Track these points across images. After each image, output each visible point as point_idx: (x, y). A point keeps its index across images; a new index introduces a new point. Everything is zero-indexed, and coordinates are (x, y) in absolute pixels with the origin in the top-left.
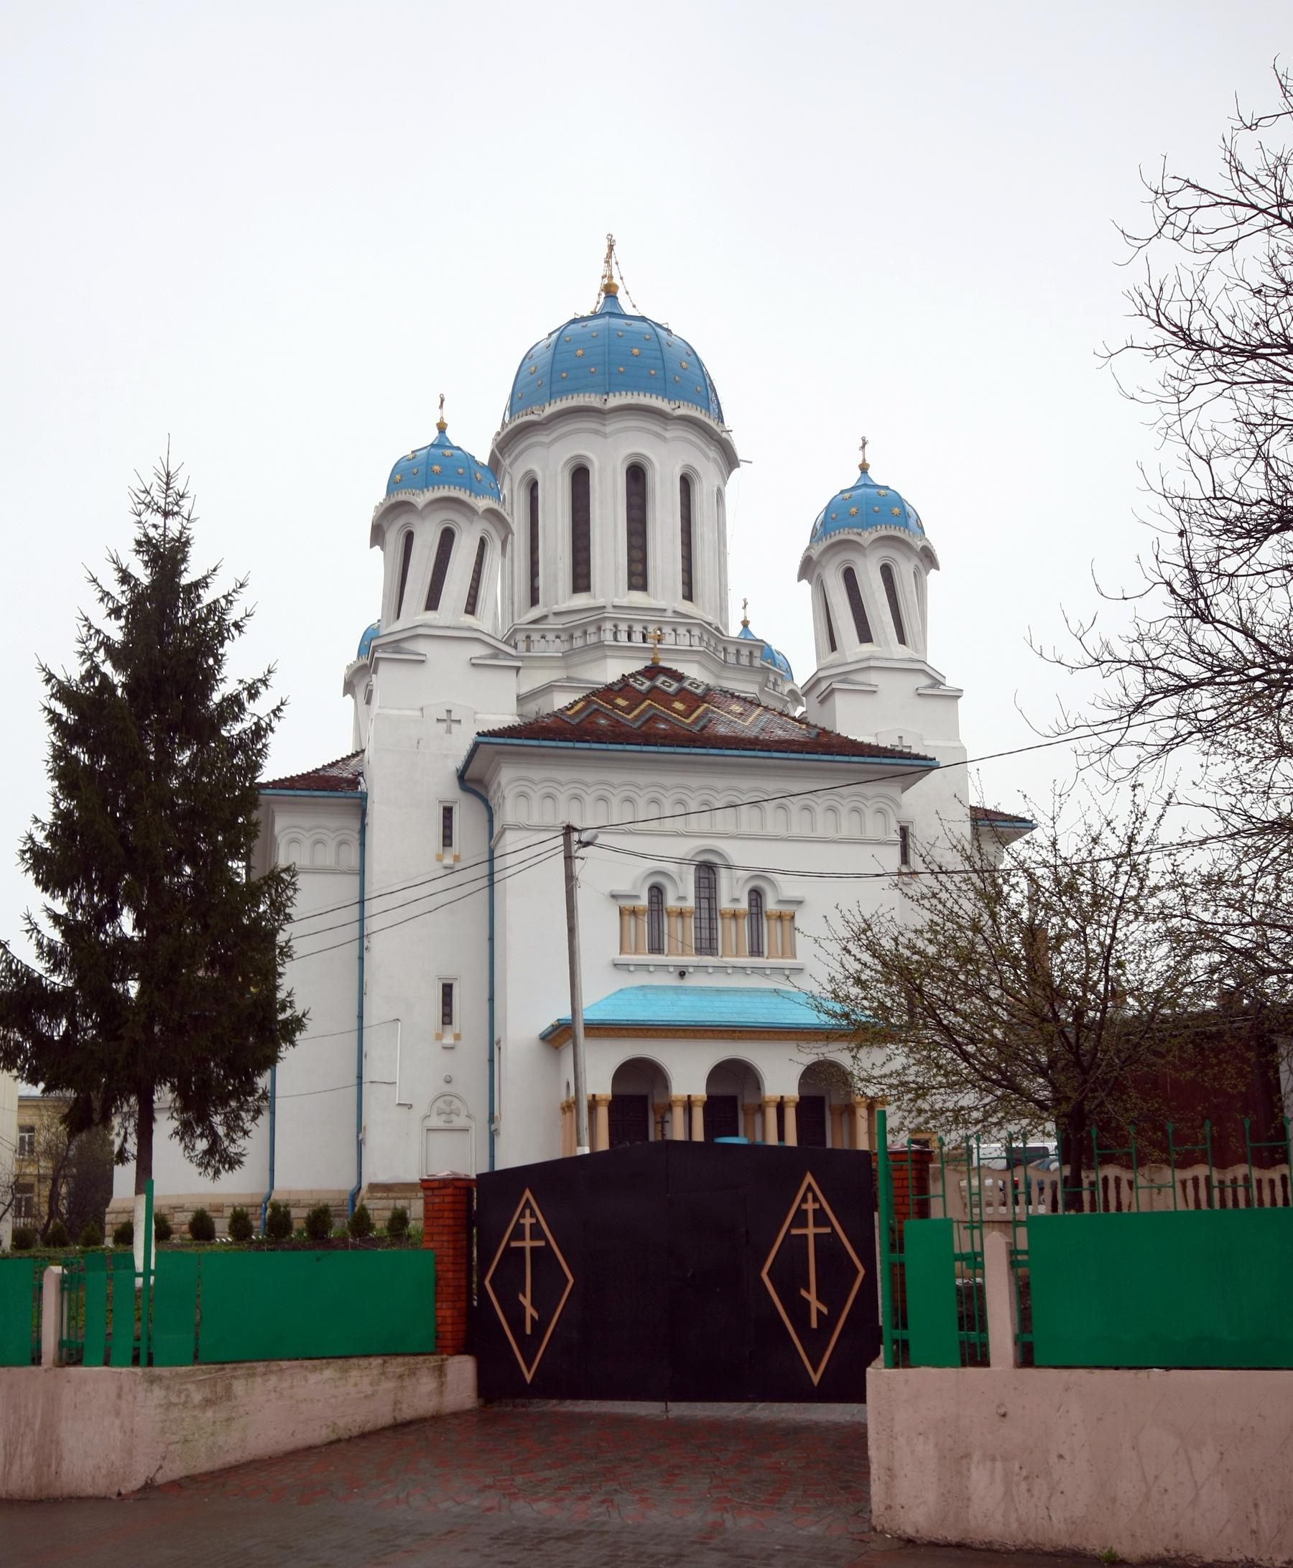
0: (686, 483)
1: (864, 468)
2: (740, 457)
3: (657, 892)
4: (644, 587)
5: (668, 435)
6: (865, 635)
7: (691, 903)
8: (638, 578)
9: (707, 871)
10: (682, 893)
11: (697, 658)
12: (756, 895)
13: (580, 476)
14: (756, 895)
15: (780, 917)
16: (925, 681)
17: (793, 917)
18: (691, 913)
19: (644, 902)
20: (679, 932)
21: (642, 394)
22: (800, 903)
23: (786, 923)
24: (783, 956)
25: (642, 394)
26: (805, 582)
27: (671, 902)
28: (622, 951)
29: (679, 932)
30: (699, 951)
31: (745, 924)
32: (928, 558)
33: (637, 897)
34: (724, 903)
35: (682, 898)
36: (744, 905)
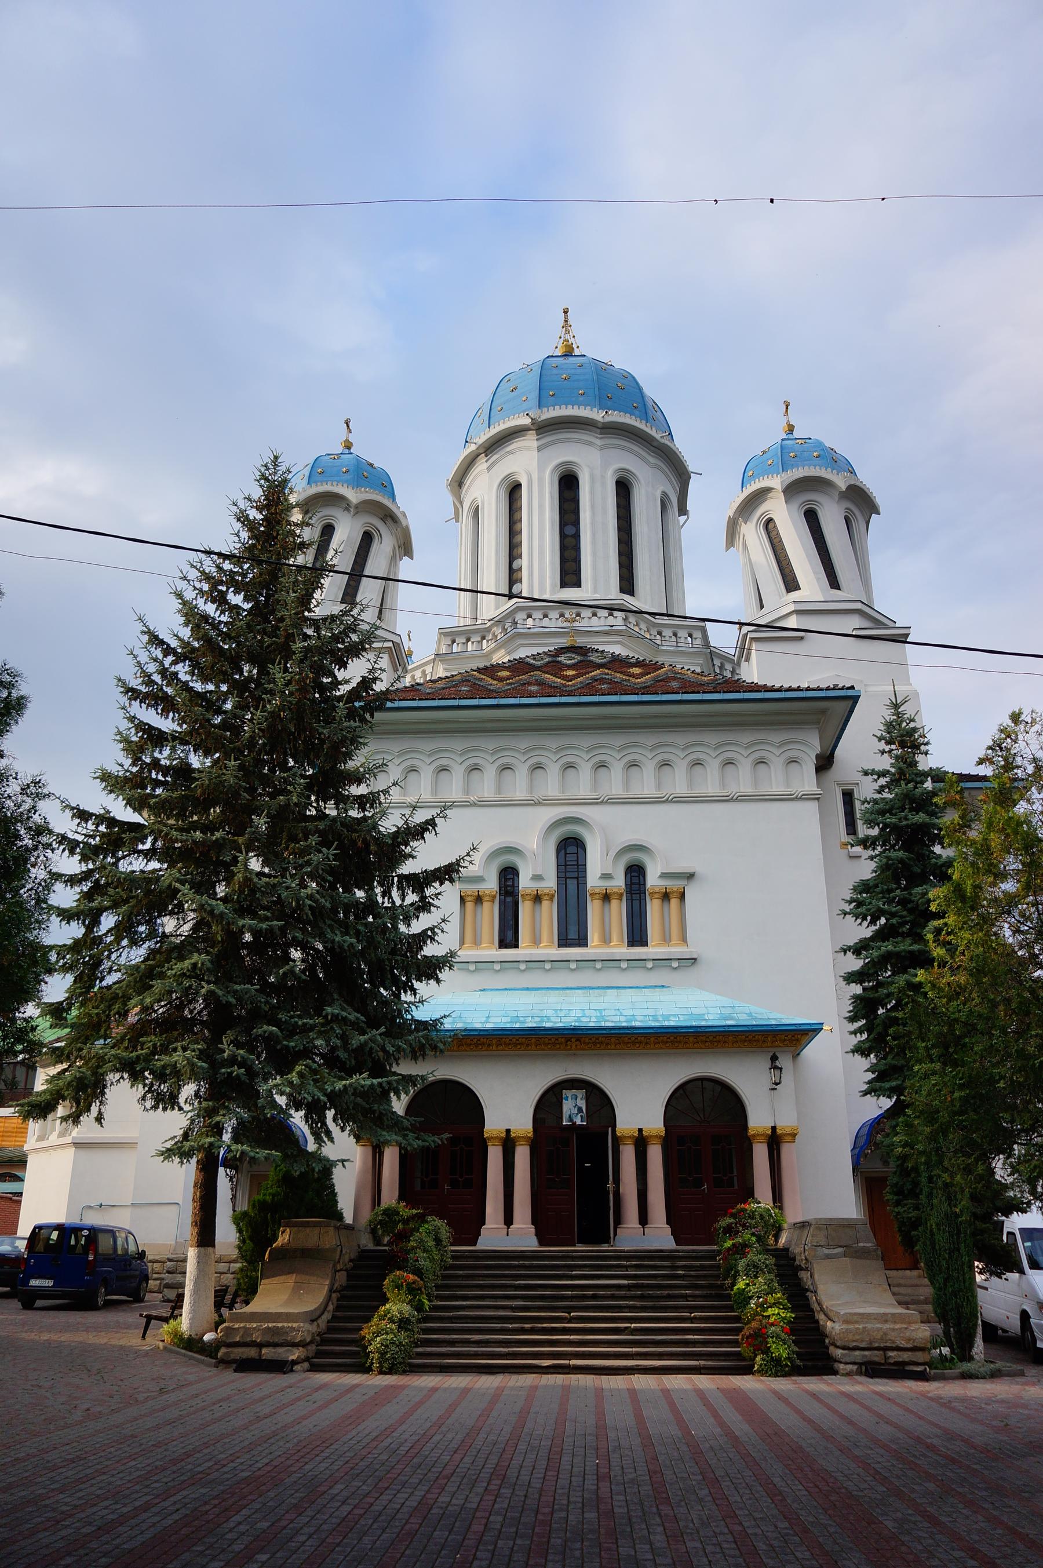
0: (624, 488)
2: (690, 469)
3: (508, 875)
4: (578, 584)
6: (791, 584)
7: (550, 883)
8: (570, 572)
10: (538, 871)
12: (636, 873)
13: (514, 490)
14: (636, 873)
15: (666, 896)
17: (682, 896)
19: (491, 884)
20: (539, 922)
22: (690, 876)
23: (674, 902)
27: (525, 883)
29: (539, 922)
30: (564, 941)
31: (618, 910)
32: (860, 502)
33: (479, 879)
34: (593, 880)
36: (619, 882)
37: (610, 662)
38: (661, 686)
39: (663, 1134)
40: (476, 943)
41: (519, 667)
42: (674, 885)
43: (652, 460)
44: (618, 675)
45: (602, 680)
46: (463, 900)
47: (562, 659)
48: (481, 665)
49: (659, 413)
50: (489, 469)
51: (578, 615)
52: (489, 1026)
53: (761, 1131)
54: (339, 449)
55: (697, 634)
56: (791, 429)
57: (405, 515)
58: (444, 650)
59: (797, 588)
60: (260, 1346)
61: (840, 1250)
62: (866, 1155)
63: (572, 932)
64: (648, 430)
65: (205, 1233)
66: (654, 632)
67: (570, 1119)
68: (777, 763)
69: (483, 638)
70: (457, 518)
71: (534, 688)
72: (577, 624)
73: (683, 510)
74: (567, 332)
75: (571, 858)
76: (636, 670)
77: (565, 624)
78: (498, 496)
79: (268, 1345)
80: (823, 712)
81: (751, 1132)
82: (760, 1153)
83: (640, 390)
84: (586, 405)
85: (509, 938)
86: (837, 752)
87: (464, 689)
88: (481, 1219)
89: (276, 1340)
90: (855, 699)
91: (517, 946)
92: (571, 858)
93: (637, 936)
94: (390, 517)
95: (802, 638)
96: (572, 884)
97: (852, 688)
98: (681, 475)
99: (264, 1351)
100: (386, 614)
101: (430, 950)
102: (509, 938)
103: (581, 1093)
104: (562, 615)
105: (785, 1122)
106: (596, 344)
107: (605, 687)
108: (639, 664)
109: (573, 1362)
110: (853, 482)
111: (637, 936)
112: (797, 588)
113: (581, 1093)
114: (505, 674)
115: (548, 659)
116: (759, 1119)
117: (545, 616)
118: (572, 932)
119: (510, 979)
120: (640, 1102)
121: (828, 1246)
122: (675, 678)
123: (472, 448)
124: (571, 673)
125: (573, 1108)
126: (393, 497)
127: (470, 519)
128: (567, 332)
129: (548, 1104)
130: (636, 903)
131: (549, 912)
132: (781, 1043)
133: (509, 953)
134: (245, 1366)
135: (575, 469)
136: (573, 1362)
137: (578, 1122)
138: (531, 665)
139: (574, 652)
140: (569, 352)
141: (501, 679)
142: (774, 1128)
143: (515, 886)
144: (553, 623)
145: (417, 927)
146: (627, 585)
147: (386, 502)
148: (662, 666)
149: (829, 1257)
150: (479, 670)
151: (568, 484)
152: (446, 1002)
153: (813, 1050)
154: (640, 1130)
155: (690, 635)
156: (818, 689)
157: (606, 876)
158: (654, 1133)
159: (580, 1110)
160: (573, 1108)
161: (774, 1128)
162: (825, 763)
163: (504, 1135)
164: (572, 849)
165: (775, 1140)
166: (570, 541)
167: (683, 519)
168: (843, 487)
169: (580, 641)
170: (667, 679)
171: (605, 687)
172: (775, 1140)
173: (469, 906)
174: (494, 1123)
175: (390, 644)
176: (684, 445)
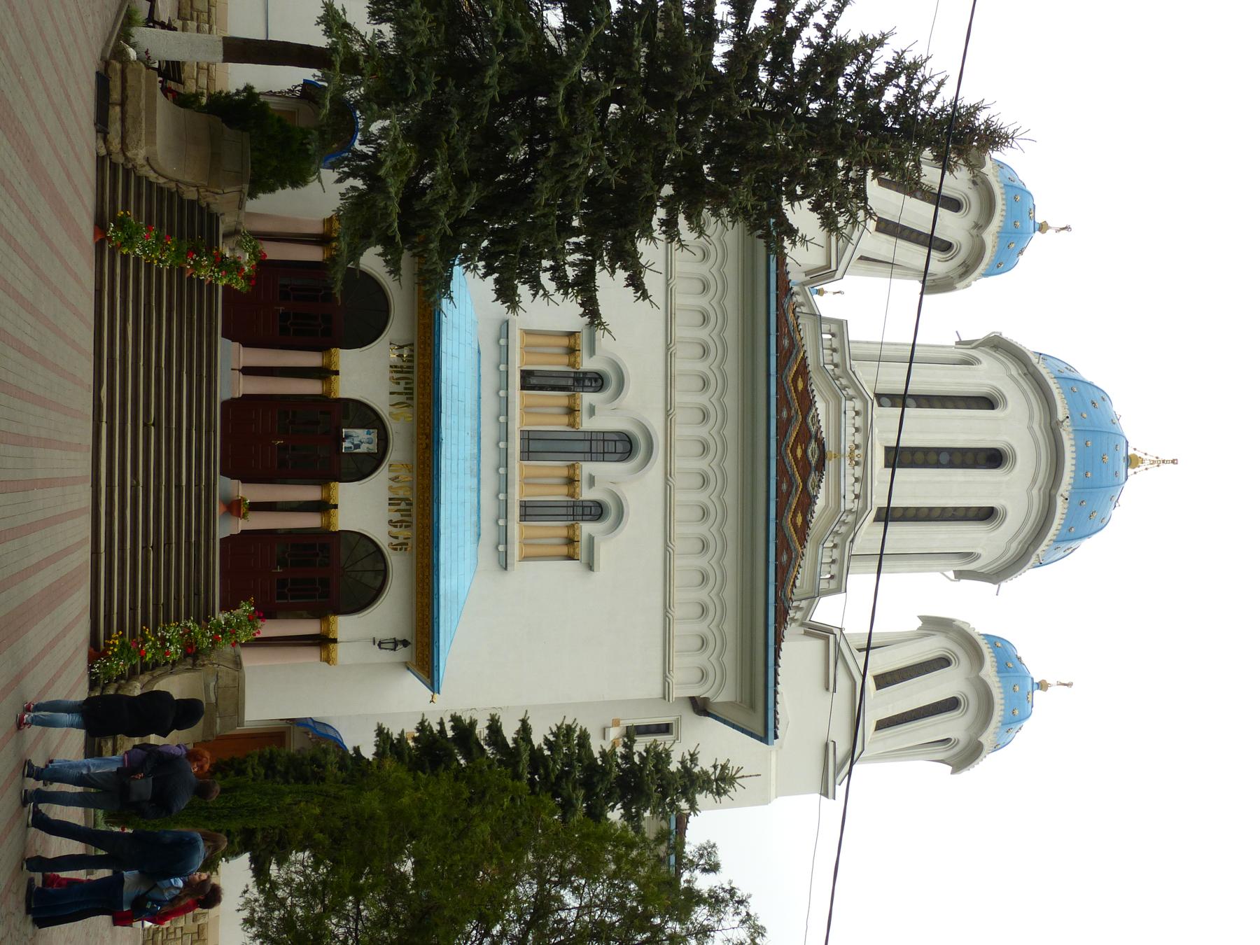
0: (986, 515)
1: (1042, 686)
2: (1003, 584)
3: (597, 381)
5: (1035, 492)
7: (587, 424)
8: (898, 457)
9: (622, 446)
10: (600, 414)
11: (832, 504)
12: (596, 511)
13: (986, 402)
14: (596, 511)
15: (571, 541)
16: (843, 748)
17: (570, 557)
18: (572, 425)
19: (587, 364)
21: (1074, 462)
22: (590, 566)
23: (564, 550)
24: (525, 543)
25: (1074, 462)
26: (919, 623)
27: (587, 398)
28: (528, 333)
30: (527, 437)
31: (559, 495)
32: (965, 756)
33: (592, 352)
34: (587, 468)
35: (592, 411)
36: (587, 494)
37: (809, 494)
38: (784, 545)
39: (332, 529)
40: (527, 349)
41: (807, 402)
42: (582, 549)
43: (1014, 545)
44: (795, 502)
45: (791, 485)
46: (571, 334)
47: (813, 445)
48: (809, 361)
49: (1063, 554)
50: (1011, 377)
51: (857, 463)
52: (443, 356)
53: (333, 627)
54: (1039, 220)
55: (833, 584)
56: (1042, 686)
57: (967, 286)
58: (825, 327)
59: (879, 687)
60: (123, 104)
61: (213, 699)
62: (307, 733)
63: (534, 446)
64: (1046, 542)
65: (240, 50)
66: (837, 540)
67: (347, 437)
68: (701, 659)
69: (836, 366)
70: (960, 343)
71: (785, 414)
72: (848, 462)
73: (960, 575)
74: (1153, 463)
75: (611, 447)
76: (799, 520)
77: (848, 449)
78: (982, 385)
79: (123, 112)
80: (752, 706)
81: (332, 618)
82: (310, 627)
83: (1088, 535)
84: (1074, 478)
85: (530, 380)
86: (710, 720)
87: (786, 342)
88: (249, 342)
89: (129, 121)
90: (764, 739)
91: (523, 388)
92: (611, 447)
93: (529, 511)
94: (967, 270)
95: (827, 689)
96: (585, 446)
97: (776, 737)
98: (998, 574)
99: (118, 109)
100: (864, 265)
101: (524, 290)
102: (530, 380)
103: (373, 448)
104: (857, 447)
105: (341, 652)
106: (1137, 490)
107: (784, 487)
108: (806, 523)
109: (104, 426)
110: (986, 748)
111: (529, 511)
112: (879, 687)
113: (373, 448)
114: (800, 385)
115: (813, 430)
116: (345, 626)
117: (857, 430)
118: (534, 446)
119: (490, 380)
120: (361, 508)
121: (217, 687)
122: (790, 558)
123: (1034, 360)
124: (799, 452)
125: (359, 439)
126: (986, 275)
127: (960, 357)
128: (1153, 463)
129: (364, 414)
130: (563, 511)
131: (557, 424)
132: (421, 650)
133: (516, 380)
134: (102, 82)
135: (1009, 465)
136: (104, 426)
137: (346, 444)
138: (808, 413)
139: (819, 457)
140: (1132, 461)
141: (795, 381)
142: (335, 641)
143: (584, 388)
144: (849, 438)
145: (545, 278)
146: (887, 516)
147: (982, 267)
148: (803, 545)
149: (207, 687)
150: (804, 359)
151: (993, 458)
152: (470, 297)
153: (412, 685)
154: (336, 507)
155: (832, 577)
156: (776, 702)
157: (592, 481)
158: (333, 520)
159: (357, 446)
160: (359, 439)
161: (335, 641)
162: (700, 707)
163: (333, 368)
164: (620, 447)
165: (323, 642)
166: (932, 458)
167: (951, 574)
168: (982, 739)
169: (830, 465)
170: (789, 550)
171: (784, 487)
172: (323, 642)
173: (565, 342)
174: (346, 359)
175: (834, 267)
176: (1028, 578)
